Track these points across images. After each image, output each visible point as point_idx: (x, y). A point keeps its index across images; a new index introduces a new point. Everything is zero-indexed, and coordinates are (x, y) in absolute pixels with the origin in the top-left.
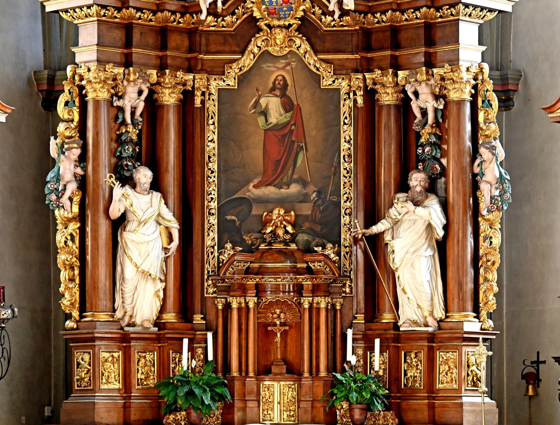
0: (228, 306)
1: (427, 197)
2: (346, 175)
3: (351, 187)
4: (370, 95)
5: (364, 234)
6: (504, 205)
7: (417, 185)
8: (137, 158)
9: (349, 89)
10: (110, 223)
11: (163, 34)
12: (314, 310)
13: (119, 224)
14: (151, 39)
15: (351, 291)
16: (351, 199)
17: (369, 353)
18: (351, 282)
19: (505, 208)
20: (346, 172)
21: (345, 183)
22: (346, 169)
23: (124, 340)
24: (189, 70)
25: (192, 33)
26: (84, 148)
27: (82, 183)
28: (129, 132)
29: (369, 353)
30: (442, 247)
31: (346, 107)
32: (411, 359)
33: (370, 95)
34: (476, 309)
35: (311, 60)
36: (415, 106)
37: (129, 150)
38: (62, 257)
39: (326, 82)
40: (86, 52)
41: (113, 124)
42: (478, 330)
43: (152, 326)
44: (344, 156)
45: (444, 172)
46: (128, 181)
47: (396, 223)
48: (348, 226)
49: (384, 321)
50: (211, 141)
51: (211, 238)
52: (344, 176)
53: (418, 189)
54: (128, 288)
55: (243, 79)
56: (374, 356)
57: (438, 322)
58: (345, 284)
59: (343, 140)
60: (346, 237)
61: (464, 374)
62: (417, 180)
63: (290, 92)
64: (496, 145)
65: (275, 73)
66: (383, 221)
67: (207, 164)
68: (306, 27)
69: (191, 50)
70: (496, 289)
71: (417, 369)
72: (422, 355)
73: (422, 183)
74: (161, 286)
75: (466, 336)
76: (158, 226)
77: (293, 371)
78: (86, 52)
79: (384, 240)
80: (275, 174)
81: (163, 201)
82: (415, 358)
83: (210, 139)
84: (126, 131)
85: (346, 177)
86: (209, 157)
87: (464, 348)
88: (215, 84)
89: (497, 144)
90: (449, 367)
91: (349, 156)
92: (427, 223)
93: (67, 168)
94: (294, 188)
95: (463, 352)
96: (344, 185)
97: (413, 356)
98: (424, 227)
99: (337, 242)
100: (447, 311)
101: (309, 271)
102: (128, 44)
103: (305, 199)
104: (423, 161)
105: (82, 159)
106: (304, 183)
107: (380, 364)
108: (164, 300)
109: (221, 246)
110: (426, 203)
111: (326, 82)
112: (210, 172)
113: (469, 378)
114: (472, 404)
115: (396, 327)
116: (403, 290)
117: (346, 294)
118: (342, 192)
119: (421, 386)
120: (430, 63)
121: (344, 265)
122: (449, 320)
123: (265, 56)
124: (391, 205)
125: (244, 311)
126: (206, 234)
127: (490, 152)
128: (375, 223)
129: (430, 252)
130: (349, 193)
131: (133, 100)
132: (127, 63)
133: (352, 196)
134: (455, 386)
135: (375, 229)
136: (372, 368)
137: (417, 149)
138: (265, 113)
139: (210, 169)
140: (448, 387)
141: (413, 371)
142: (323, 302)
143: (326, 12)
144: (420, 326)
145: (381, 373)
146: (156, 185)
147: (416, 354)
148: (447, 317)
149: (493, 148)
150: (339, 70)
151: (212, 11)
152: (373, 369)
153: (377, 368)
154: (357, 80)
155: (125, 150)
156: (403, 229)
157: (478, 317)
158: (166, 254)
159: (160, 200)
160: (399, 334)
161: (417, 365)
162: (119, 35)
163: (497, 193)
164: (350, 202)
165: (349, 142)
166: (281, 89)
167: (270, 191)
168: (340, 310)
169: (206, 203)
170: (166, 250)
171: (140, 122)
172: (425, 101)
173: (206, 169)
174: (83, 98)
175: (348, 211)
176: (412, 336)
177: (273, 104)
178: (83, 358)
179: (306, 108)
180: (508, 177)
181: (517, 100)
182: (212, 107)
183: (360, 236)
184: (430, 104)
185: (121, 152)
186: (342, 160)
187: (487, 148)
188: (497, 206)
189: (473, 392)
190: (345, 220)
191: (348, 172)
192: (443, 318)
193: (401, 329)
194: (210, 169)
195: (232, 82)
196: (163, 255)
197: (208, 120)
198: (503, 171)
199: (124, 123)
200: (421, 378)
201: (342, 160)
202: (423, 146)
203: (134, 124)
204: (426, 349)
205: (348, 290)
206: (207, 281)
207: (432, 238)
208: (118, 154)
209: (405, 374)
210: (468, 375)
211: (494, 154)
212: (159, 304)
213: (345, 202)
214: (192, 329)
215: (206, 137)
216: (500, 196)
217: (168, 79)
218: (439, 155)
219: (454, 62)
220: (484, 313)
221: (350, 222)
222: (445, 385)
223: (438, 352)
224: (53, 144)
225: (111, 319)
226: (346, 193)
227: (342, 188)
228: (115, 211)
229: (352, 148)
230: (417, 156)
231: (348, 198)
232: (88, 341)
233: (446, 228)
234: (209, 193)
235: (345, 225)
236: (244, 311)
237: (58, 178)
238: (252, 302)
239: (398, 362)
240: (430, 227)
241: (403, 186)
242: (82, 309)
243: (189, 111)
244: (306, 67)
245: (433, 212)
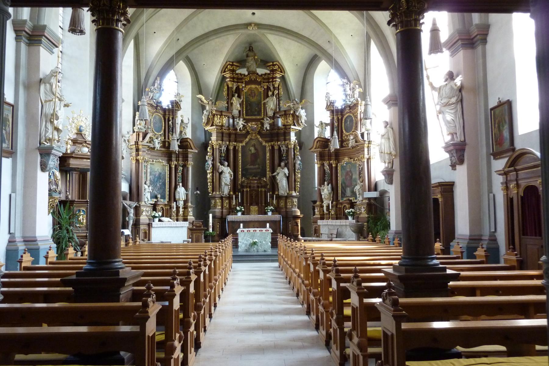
0: (243, 191)
4: (273, 147)
8: (224, 160)
9: (268, 146)
11: (229, 135)
12: (261, 191)
13: (221, 173)
14: (227, 136)
23: (222, 198)
24: (235, 142)
25: (236, 134)
26: (213, 158)
27: (213, 165)
30: (288, 178)
31: (268, 149)
33: (273, 147)
34: (295, 191)
35: (260, 139)
36: (282, 149)
37: (223, 158)
38: (209, 181)
39: (264, 144)
40: (214, 138)
45: (288, 162)
46: (222, 164)
47: (278, 174)
51: (240, 176)
54: (223, 187)
55: (246, 144)
60: (268, 176)
62: (283, 164)
63: (256, 146)
65: (253, 142)
68: (259, 133)
69: (236, 137)
77: (257, 204)
78: (214, 138)
80: (253, 163)
88: (240, 145)
93: (210, 162)
94: (257, 166)
99: (266, 177)
101: (260, 183)
102: (223, 136)
103: (259, 168)
105: (213, 160)
106: (259, 164)
109: (242, 178)
111: (264, 144)
120: (285, 140)
123: (251, 139)
125: (247, 191)
131: (224, 148)
132: (222, 141)
138: (251, 151)
141: (282, 204)
142: (263, 190)
143: (264, 130)
146: (228, 166)
150: (266, 142)
151: (240, 130)
154: (270, 144)
156: (280, 174)
162: (220, 135)
166: (254, 146)
167: (252, 167)
172: (284, 148)
174: (213, 148)
177: (252, 149)
178: (213, 202)
179: (259, 150)
181: (303, 149)
182: (240, 149)
184: (285, 148)
190: (268, 173)
195: (244, 144)
217: (231, 143)
219: (290, 139)
224: (207, 157)
228: (220, 171)
232: (214, 198)
233: (289, 174)
236: (247, 191)
237: (208, 164)
238: (248, 189)
240: (285, 174)
241: (279, 165)
242: (213, 191)
243: (235, 150)
244: (259, 141)
245: (286, 171)
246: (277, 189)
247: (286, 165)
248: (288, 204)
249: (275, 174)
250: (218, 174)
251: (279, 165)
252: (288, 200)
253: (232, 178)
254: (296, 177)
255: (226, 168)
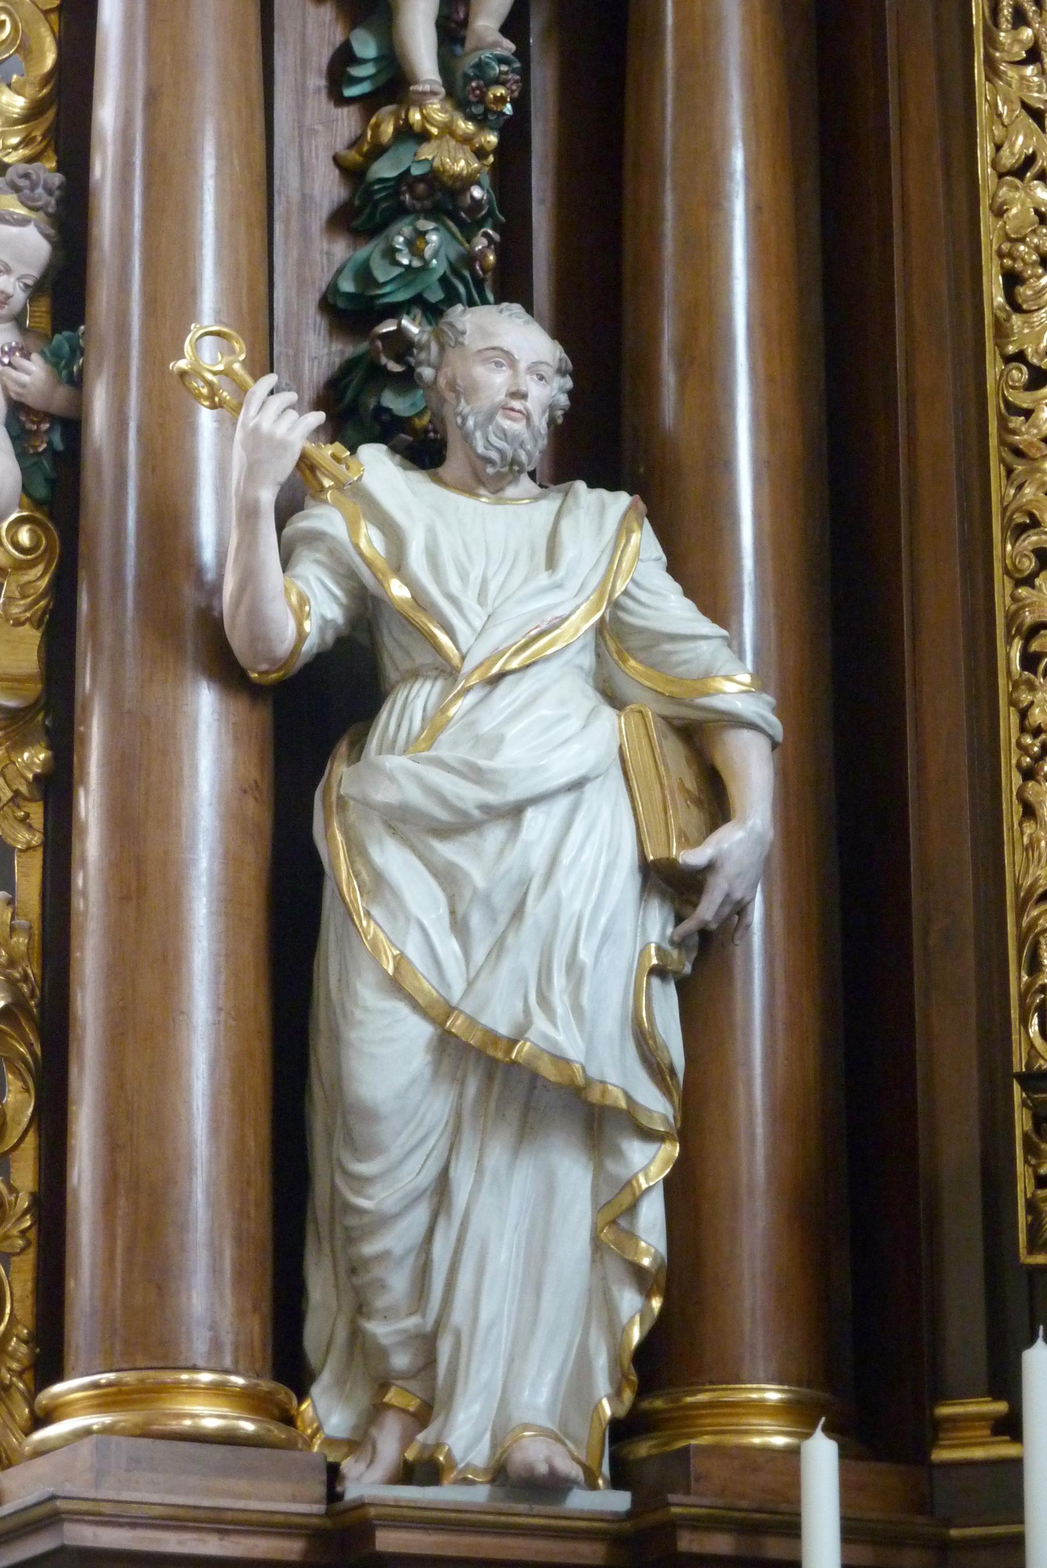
10: (263, 715)
28: (424, 137)
41: (319, 104)
43: (575, 1471)
50: (1019, 172)
67: (1002, 333)
74: (649, 1163)
76: (608, 713)
81: (645, 541)
83: (1009, 159)
84: (407, 134)
86: (1012, 280)
108: (685, 1282)
112: (1020, 375)
126: (1010, 810)
139: (1020, 357)
155: (390, 254)
158: (679, 919)
159: (624, 530)
169: (1002, 587)
170: (671, 883)
171: (501, 60)
173: (993, 368)
185: (364, 275)
194: (1020, 357)
196: (657, 924)
197: (991, 41)
199: (394, 84)
203: (462, 89)
206: (1030, 1148)
208: (347, 286)
212: (635, 1313)
214: (923, 1505)
215: (985, 151)
225: (248, 1427)
234: (1020, 518)
250: (209, 740)
253: (744, 842)
255: (523, 515)
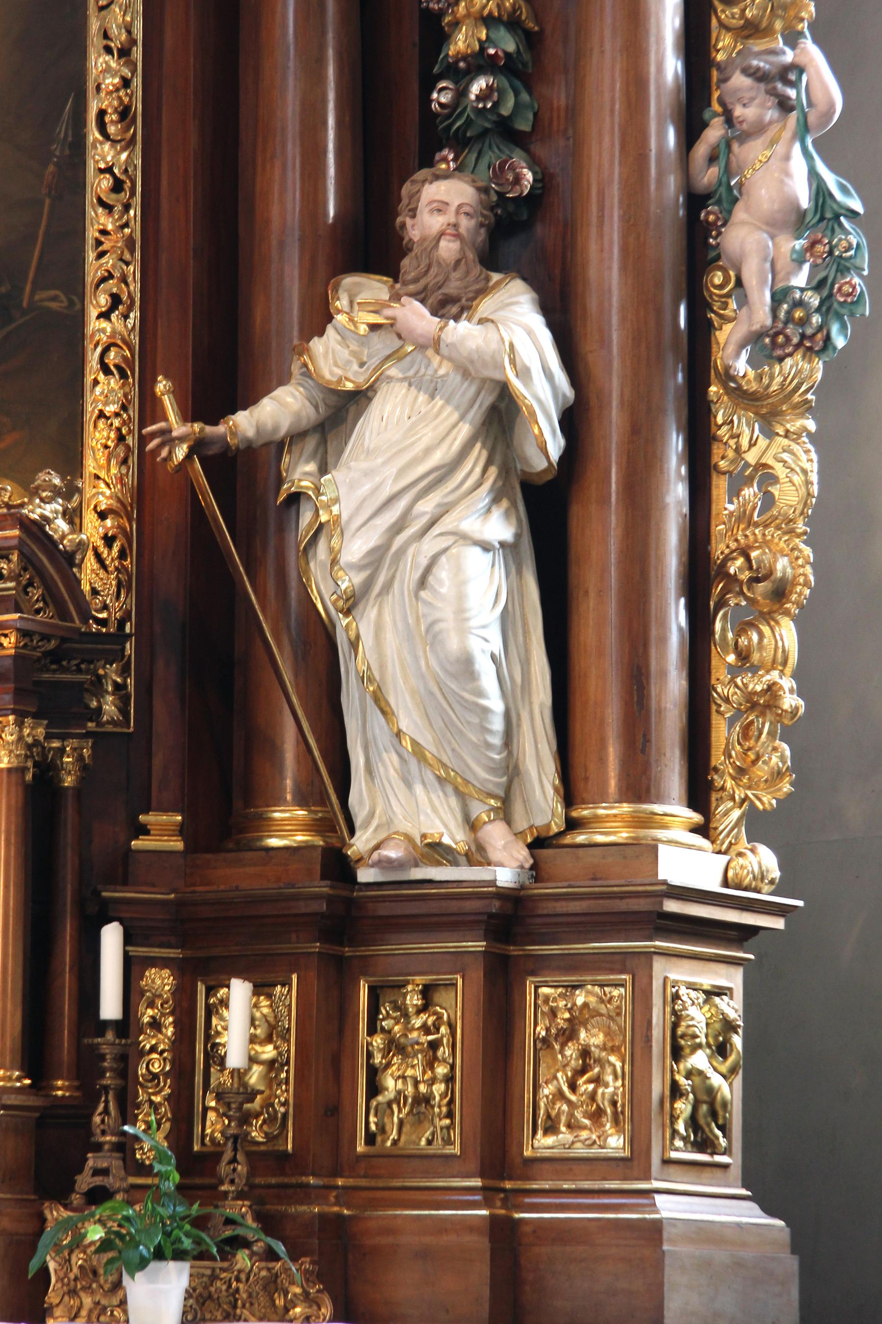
1: (483, 291)
2: (110, 199)
3: (132, 251)
5: (198, 447)
6: (835, 329)
7: (442, 234)
15: (124, 711)
16: (130, 308)
17: (201, 988)
18: (124, 671)
19: (840, 342)
20: (106, 182)
21: (104, 232)
22: (109, 170)
29: (201, 988)
30: (548, 513)
32: (406, 1015)
34: (699, 794)
42: (714, 885)
44: (102, 113)
48: (116, 422)
49: (274, 842)
52: (101, 203)
53: (448, 248)
56: (225, 1003)
57: (530, 846)
58: (99, 680)
59: (95, 41)
61: (658, 1087)
64: (802, 60)
66: (280, 392)
70: (790, 701)
71: (430, 1064)
72: (453, 1005)
73: (466, 224)
75: (672, 906)
79: (280, 481)
82: (422, 1009)
85: (109, 208)
87: (659, 966)
89: (812, 53)
90: (585, 1053)
91: (124, 113)
92: (488, 399)
95: (657, 985)
96: (99, 243)
97: (414, 1000)
98: (477, 413)
100: (569, 795)
104: (461, 143)
107: (253, 1039)
110: (486, 306)
113: (679, 1105)
114: (703, 1233)
115: (338, 865)
116: (379, 699)
117: (99, 724)
118: (93, 268)
119: (448, 1142)
121: (95, 592)
122: (581, 838)
124: (319, 319)
127: (773, 92)
128: (249, 400)
129: (500, 528)
130: (124, 280)
133: (135, 287)
134: (616, 1143)
135: (245, 423)
136: (215, 1057)
137: (428, 85)
140: (580, 1151)
144: (455, 863)
145: (255, 1077)
147: (427, 992)
148: (572, 825)
149: (789, 74)
152: (222, 1060)
153: (235, 1059)
157: (703, 830)
160: (350, 902)
161: (434, 1046)
163: (800, 279)
164: (126, 317)
165: (124, 53)
168: (78, 791)
175: (112, 357)
176: (420, 909)
180: (856, 205)
183: (181, 452)
186: (94, 134)
187: (760, 76)
188: (803, 336)
189: (692, 1173)
191: (117, 187)
192: (555, 829)
193: (365, 875)
198: (831, 180)
200: (452, 1102)
201: (94, 134)
202: (452, 71)
204: (478, 974)
205: (109, 707)
207: (505, 471)
209: (374, 1089)
210: (676, 1091)
211: (785, 106)
213: (105, 315)
216: (819, 286)
218: (524, 125)
220: (728, 816)
221: (124, 408)
222: (565, 1136)
223: (530, 989)
226: (111, 276)
227: (91, 255)
229: (137, 82)
230: (427, 116)
231: (116, 300)
233: (572, 420)
235: (101, 415)
239: (341, 1031)
246: (291, 737)
247: (523, 238)
248: (549, 1084)
249: (278, 409)
251: (372, 242)
252: (544, 998)
254: (724, 506)
